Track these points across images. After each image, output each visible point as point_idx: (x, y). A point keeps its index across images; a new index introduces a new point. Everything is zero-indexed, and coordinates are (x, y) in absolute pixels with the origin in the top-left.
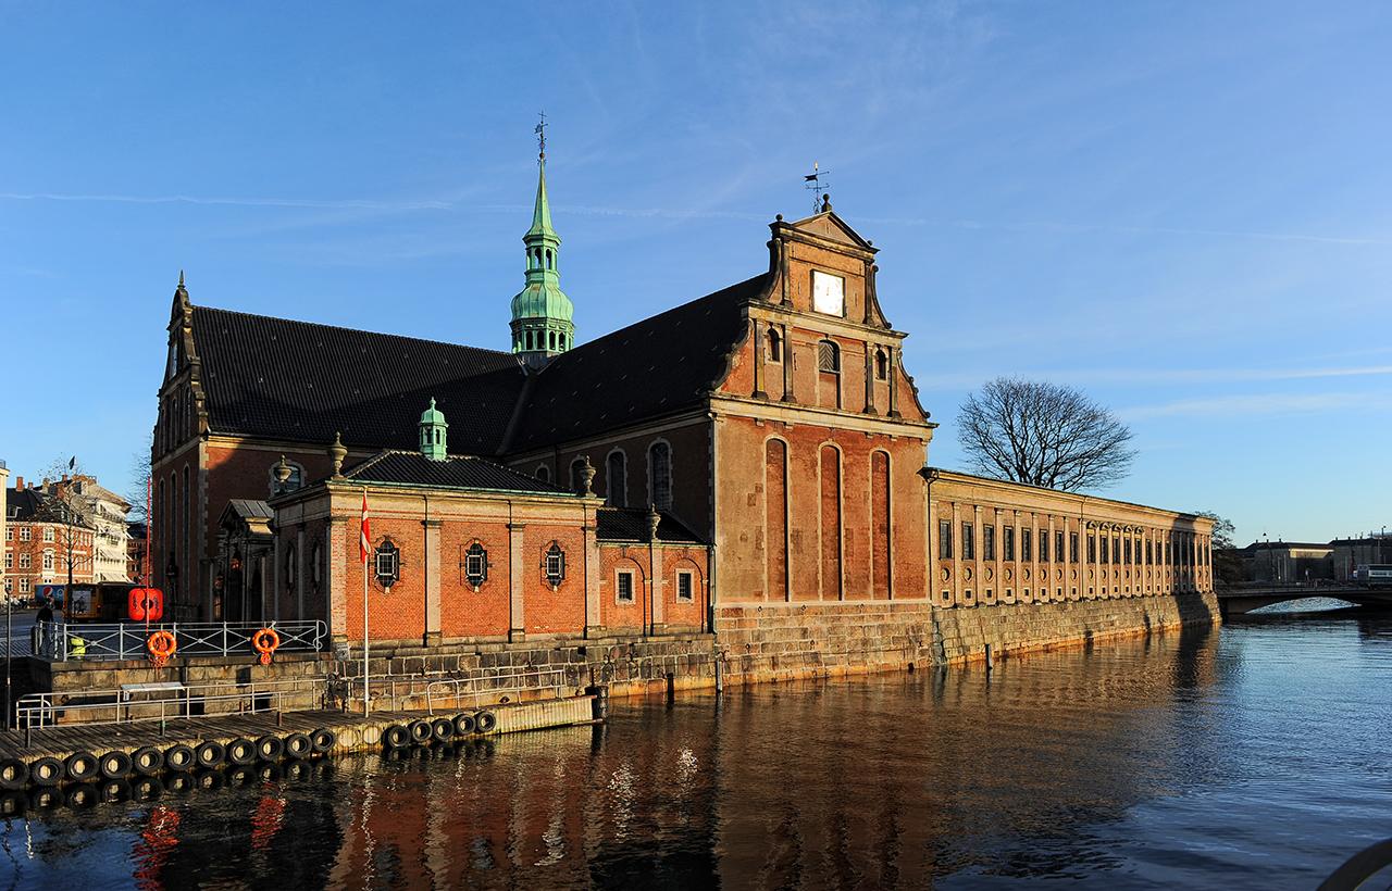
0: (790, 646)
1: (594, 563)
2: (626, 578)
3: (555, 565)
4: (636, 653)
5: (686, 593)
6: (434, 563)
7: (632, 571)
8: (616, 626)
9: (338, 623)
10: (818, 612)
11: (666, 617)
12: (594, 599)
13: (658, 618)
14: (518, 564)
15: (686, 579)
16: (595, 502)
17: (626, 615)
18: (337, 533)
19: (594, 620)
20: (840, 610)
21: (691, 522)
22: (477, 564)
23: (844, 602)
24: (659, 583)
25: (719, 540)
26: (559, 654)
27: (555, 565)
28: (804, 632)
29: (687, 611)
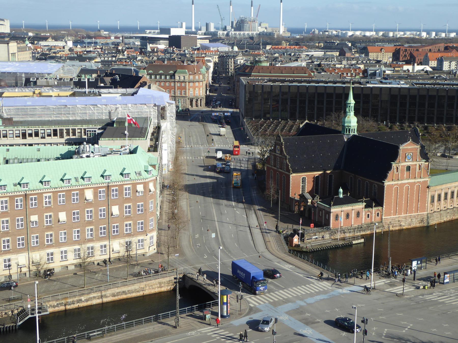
0: (396, 224)
1: (364, 214)
2: (368, 215)
3: (358, 214)
4: (369, 227)
5: (378, 215)
6: (342, 217)
7: (370, 214)
8: (367, 223)
9: (331, 226)
10: (402, 217)
11: (375, 220)
12: (363, 219)
13: (373, 221)
14: (353, 215)
15: (378, 213)
16: (365, 204)
17: (368, 220)
18: (332, 214)
19: (363, 222)
20: (406, 216)
21: (380, 203)
22: (348, 216)
23: (408, 215)
24: (374, 215)
25: (384, 206)
26: (358, 228)
27: (358, 214)
28: (399, 221)
29: (378, 218)
